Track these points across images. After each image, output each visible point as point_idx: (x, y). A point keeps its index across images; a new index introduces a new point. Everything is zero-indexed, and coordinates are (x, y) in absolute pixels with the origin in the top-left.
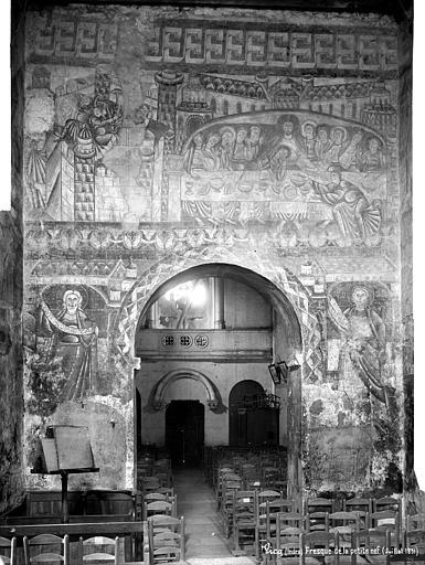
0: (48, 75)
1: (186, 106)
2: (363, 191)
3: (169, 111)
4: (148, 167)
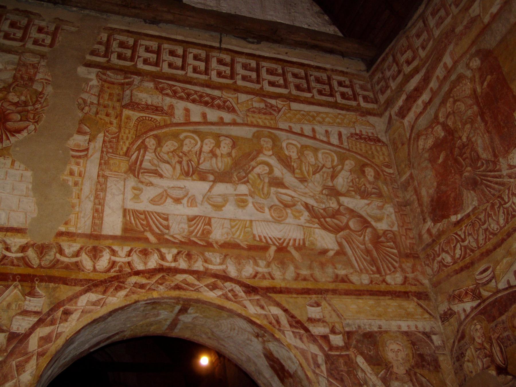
2: (369, 219)
4: (78, 164)
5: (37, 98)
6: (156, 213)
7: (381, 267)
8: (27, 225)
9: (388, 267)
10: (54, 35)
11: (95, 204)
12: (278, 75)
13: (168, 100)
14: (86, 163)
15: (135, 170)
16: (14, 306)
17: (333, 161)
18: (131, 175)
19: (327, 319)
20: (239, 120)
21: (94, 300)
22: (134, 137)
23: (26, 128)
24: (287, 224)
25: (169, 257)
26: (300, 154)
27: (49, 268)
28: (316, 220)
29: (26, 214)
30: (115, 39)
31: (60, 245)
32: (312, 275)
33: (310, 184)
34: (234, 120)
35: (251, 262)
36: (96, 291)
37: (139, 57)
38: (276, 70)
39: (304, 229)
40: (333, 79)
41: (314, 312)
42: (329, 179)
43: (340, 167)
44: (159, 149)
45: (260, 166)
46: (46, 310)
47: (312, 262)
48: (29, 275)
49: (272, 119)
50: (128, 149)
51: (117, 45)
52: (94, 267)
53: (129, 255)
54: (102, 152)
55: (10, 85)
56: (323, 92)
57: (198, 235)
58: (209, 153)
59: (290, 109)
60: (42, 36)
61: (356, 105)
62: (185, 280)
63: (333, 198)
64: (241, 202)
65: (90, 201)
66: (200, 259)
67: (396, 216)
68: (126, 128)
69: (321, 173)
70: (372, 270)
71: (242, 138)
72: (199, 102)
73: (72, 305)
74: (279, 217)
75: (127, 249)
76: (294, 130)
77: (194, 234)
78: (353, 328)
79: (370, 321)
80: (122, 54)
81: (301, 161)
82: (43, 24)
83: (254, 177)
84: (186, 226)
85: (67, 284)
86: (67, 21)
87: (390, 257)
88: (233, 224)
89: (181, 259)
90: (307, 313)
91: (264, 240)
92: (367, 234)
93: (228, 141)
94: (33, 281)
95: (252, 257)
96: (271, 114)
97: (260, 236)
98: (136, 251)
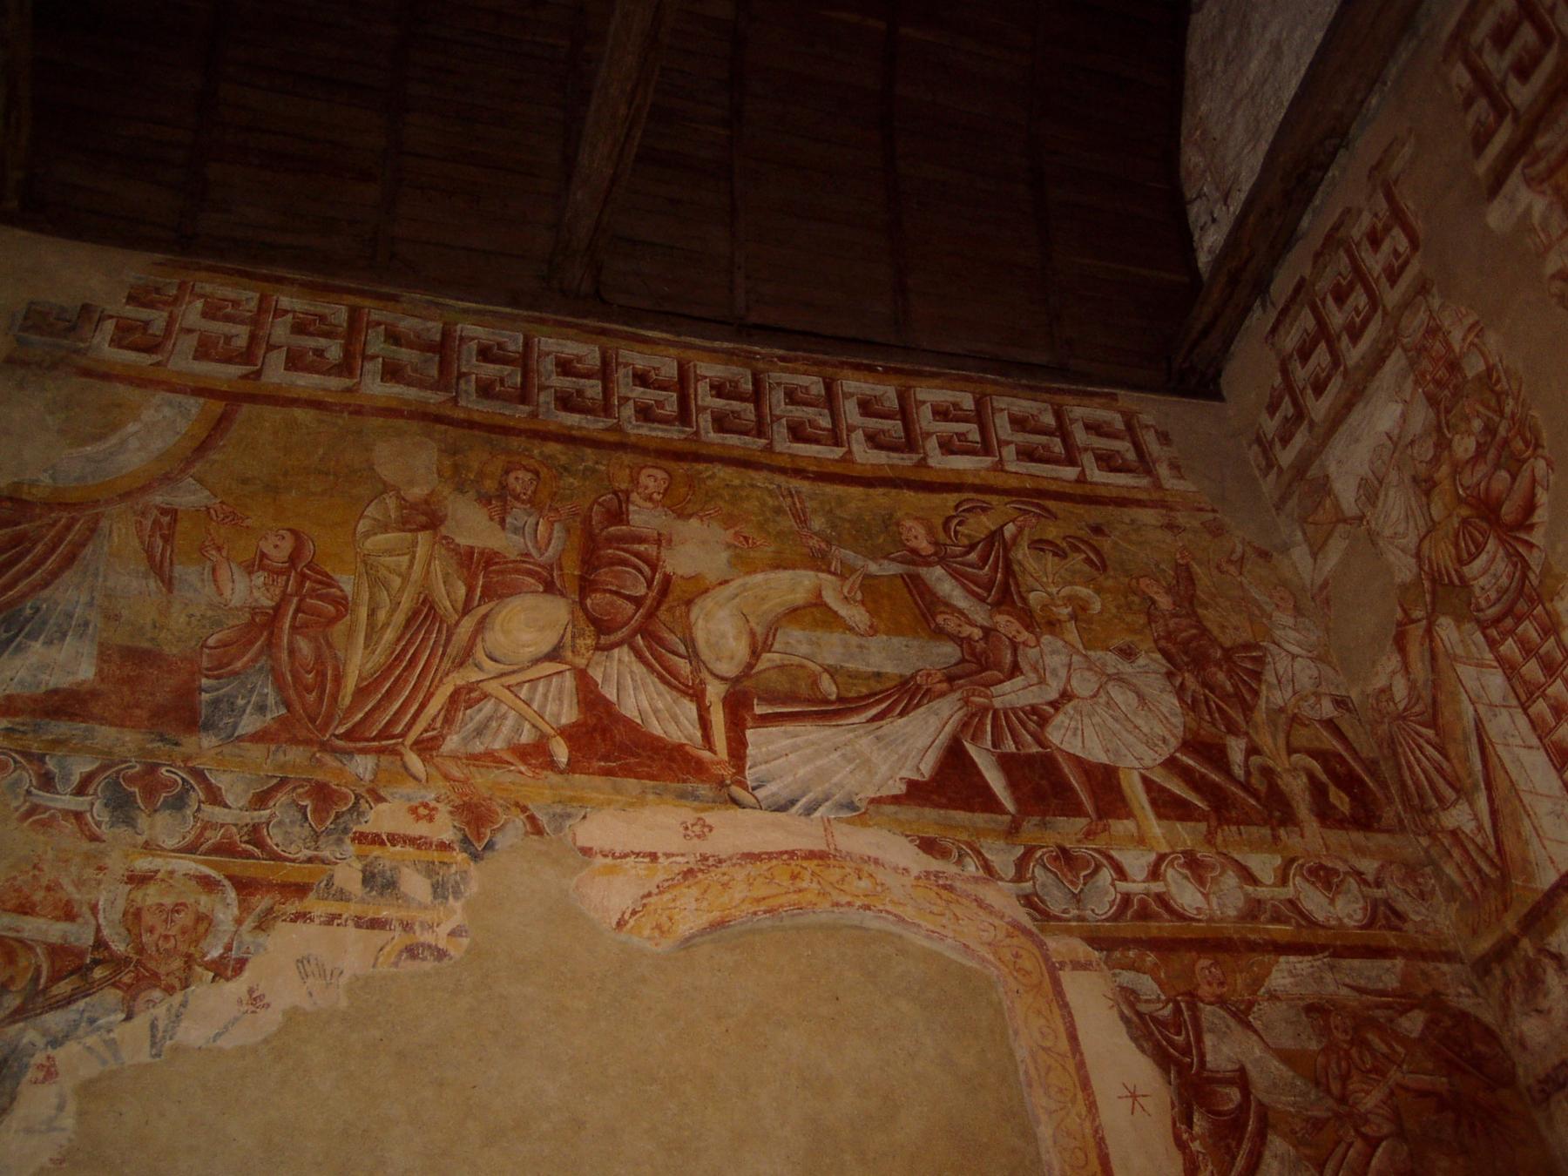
0: (1324, 486)
10: (1398, 216)
23: (1534, 481)
55: (1439, 429)
60: (1386, 247)
82: (1366, 220)
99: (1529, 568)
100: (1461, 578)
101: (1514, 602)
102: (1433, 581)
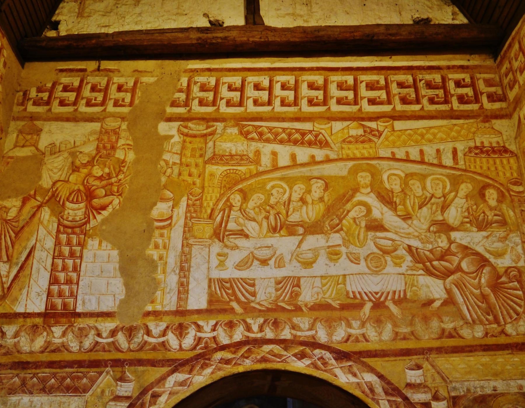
1: (217, 158)
2: (487, 255)
3: (197, 165)
4: (162, 235)
5: (120, 167)
6: (242, 279)
7: (500, 314)
8: (116, 308)
9: (508, 313)
10: (133, 90)
11: (180, 277)
12: (380, 89)
13: (255, 146)
14: (170, 233)
15: (219, 234)
16: (107, 393)
17: (444, 187)
18: (216, 240)
19: (429, 384)
20: (333, 156)
21: (181, 381)
22: (218, 195)
23: (111, 203)
24: (385, 274)
25: (255, 328)
26: (403, 186)
27: (138, 351)
28: (421, 266)
29: (114, 296)
30: (196, 83)
31: (147, 326)
32: (412, 333)
33: (415, 222)
34: (327, 156)
35: (343, 323)
36: (182, 370)
37: (222, 99)
38: (378, 82)
39: (405, 277)
40: (449, 79)
41: (414, 376)
42: (439, 212)
43: (453, 194)
44: (244, 205)
45: (357, 208)
46: (135, 396)
47: (413, 316)
48: (119, 360)
49: (371, 148)
50: (213, 210)
51: (198, 89)
52: (180, 346)
53: (214, 330)
54: (186, 218)
55: (94, 158)
56: (436, 99)
57: (286, 299)
58: (298, 201)
59: (394, 130)
60: (122, 95)
61: (477, 108)
62: (271, 350)
63: (442, 234)
64: (333, 254)
65: (176, 274)
66: (287, 327)
67: (523, 247)
68: (210, 187)
69: (429, 205)
70: (487, 320)
71: (335, 176)
72: (287, 142)
73: (160, 387)
74: (377, 267)
75: (212, 322)
76: (398, 156)
77: (282, 298)
78: (460, 393)
79: (482, 382)
80: (204, 99)
81: (405, 194)
82: (122, 80)
83: (349, 223)
84: (274, 291)
85: (155, 366)
86: (145, 72)
87: (512, 301)
88: (324, 281)
89: (267, 328)
90: (406, 378)
91: (358, 296)
92: (483, 274)
93: (321, 183)
94: (122, 366)
95: (345, 318)
96: (370, 140)
97: (353, 292)
98: (221, 325)
99: (89, 223)
100: (64, 204)
101: (76, 227)
102: (53, 195)
